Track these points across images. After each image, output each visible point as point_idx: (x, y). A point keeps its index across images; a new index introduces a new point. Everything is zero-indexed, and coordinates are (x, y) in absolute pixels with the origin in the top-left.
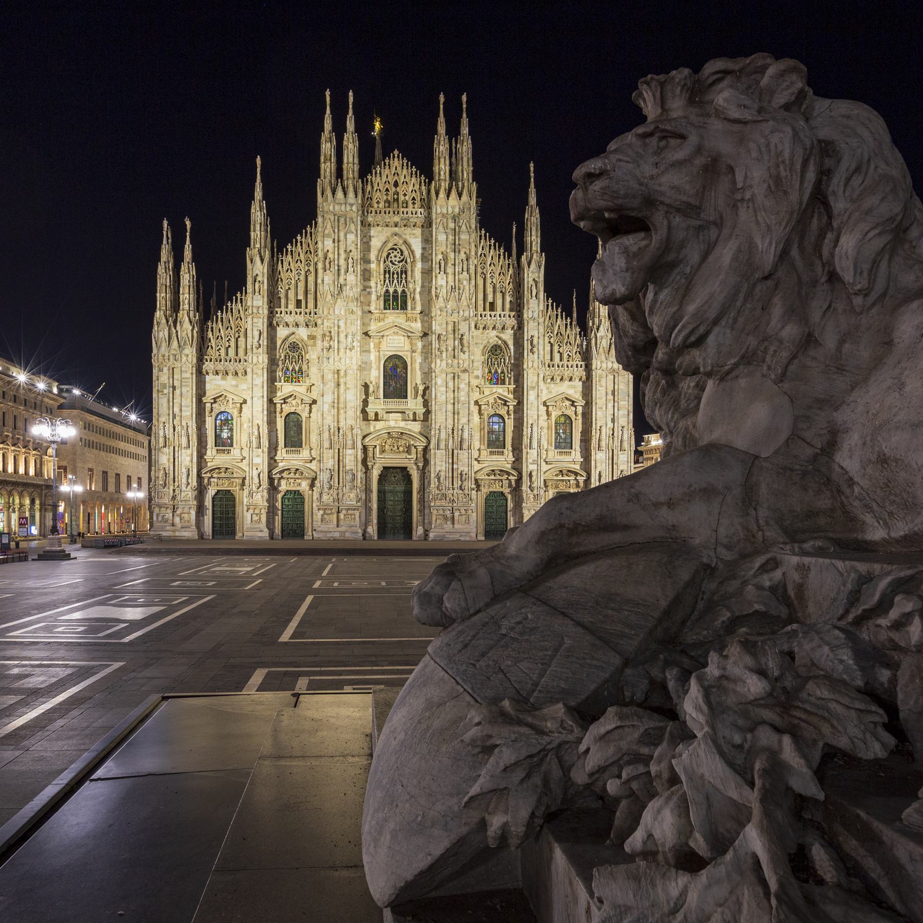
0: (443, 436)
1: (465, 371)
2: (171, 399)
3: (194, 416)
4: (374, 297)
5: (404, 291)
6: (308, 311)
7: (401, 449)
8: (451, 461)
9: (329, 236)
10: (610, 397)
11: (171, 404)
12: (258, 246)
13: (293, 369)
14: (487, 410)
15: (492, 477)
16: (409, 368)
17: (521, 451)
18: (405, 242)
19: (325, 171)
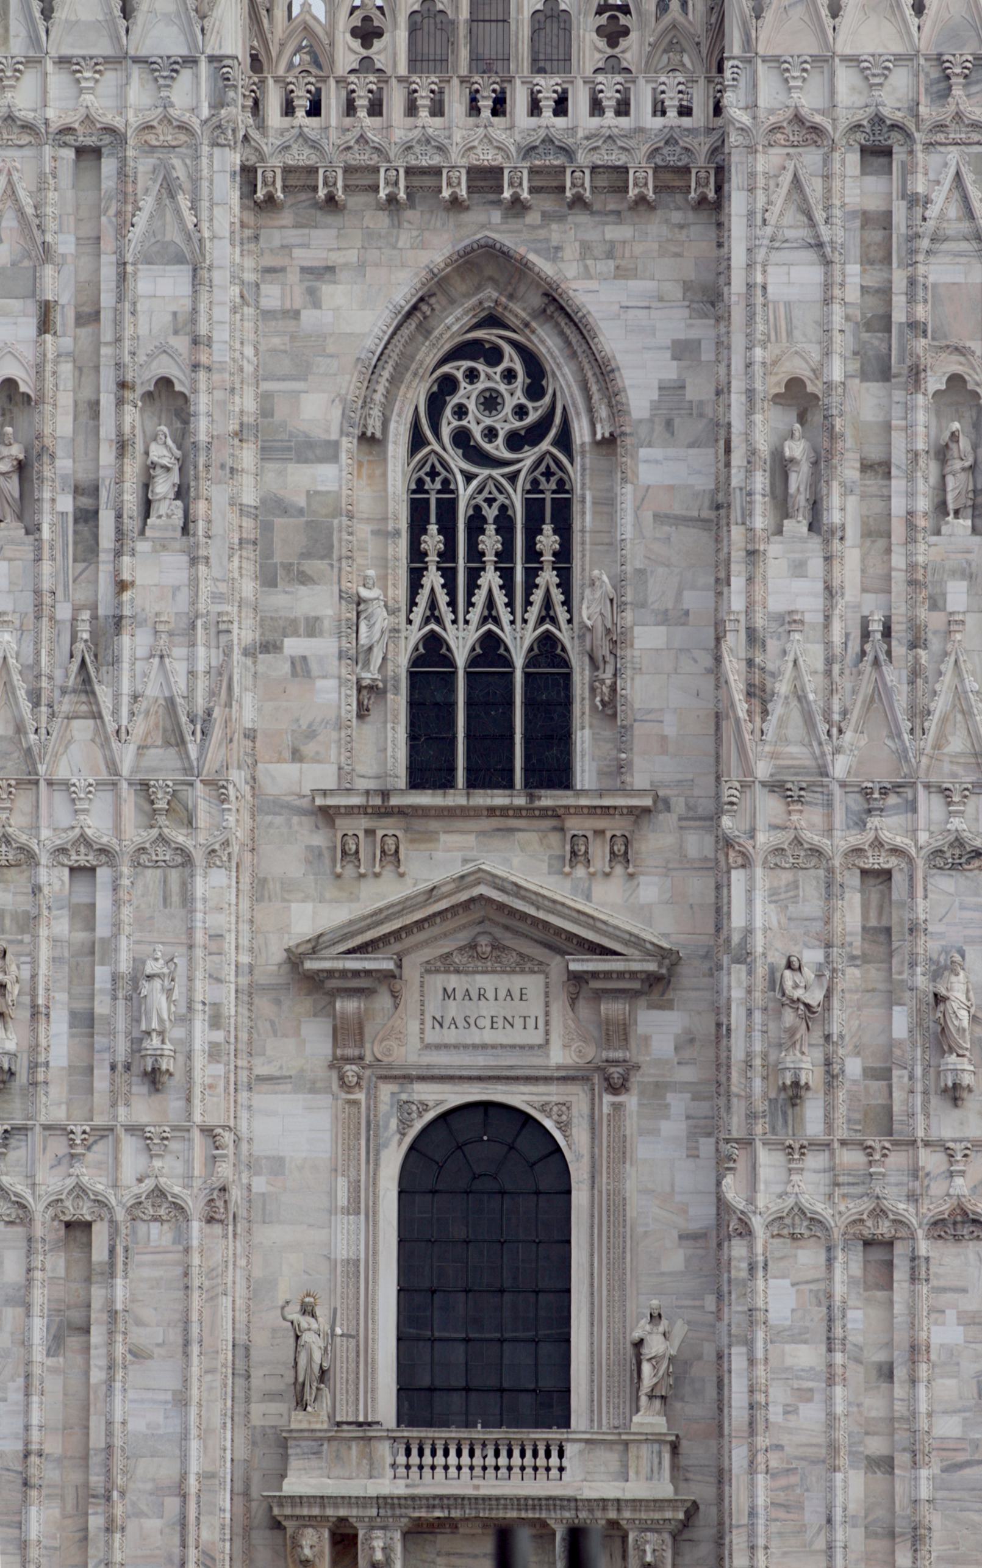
4: (331, 694)
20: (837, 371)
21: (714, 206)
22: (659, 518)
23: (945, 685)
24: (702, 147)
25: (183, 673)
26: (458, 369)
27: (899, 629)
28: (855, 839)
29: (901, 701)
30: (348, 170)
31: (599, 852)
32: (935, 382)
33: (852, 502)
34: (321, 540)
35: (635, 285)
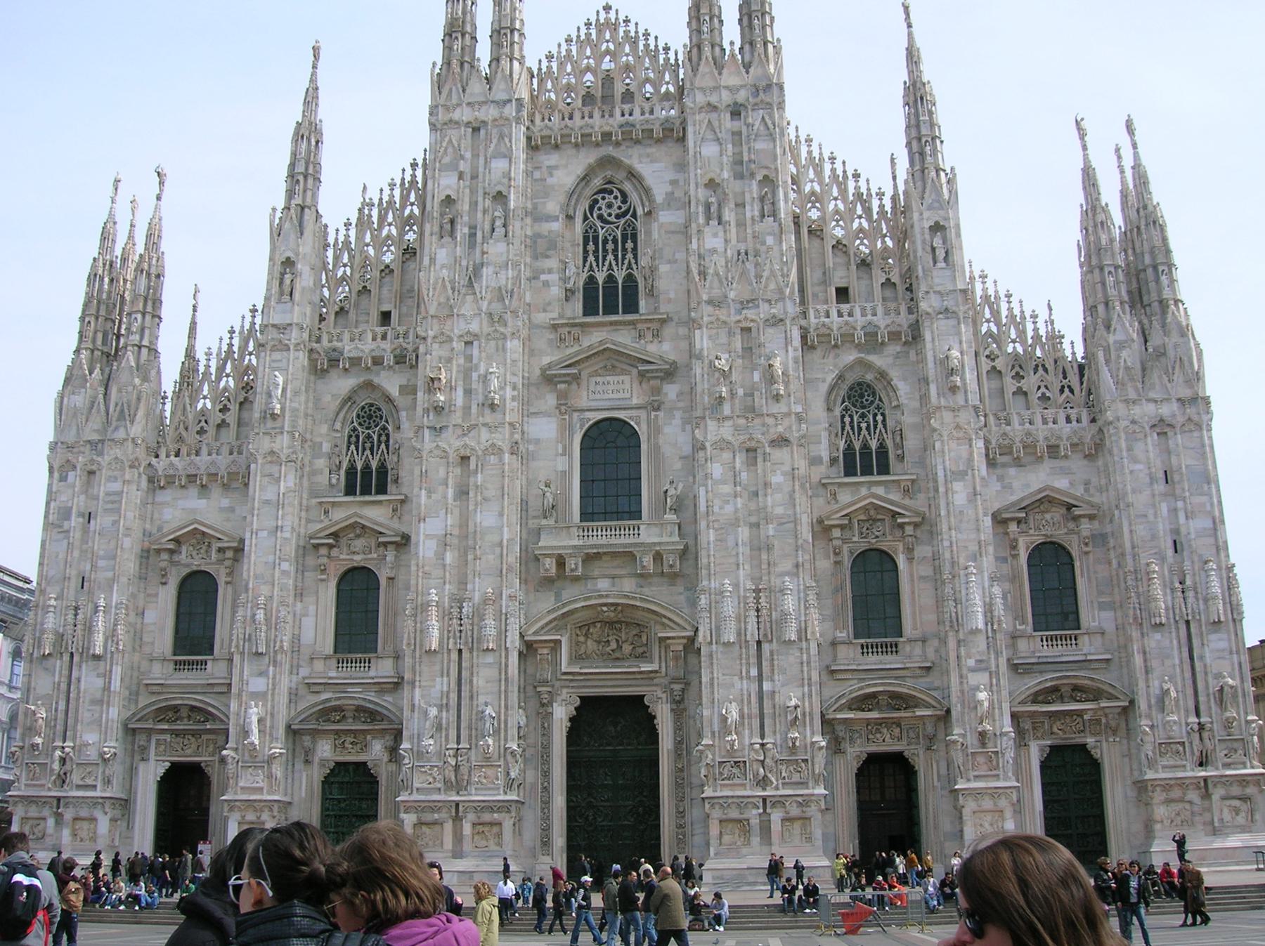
0: (729, 608)
1: (781, 441)
2: (77, 543)
3: (124, 580)
4: (556, 291)
5: (630, 278)
6: (401, 329)
7: (627, 648)
8: (754, 672)
9: (453, 166)
10: (1160, 487)
11: (76, 554)
12: (297, 200)
13: (367, 467)
14: (844, 541)
15: (874, 715)
16: (644, 447)
17: (943, 641)
18: (632, 175)
19: (451, 49)
20: (726, 175)
21: (682, 139)
22: (667, 232)
23: (767, 267)
24: (678, 123)
25: (505, 278)
26: (599, 197)
27: (751, 253)
28: (738, 318)
29: (752, 274)
30: (562, 136)
31: (649, 337)
32: (759, 177)
33: (733, 214)
34: (552, 245)
35: (657, 166)
